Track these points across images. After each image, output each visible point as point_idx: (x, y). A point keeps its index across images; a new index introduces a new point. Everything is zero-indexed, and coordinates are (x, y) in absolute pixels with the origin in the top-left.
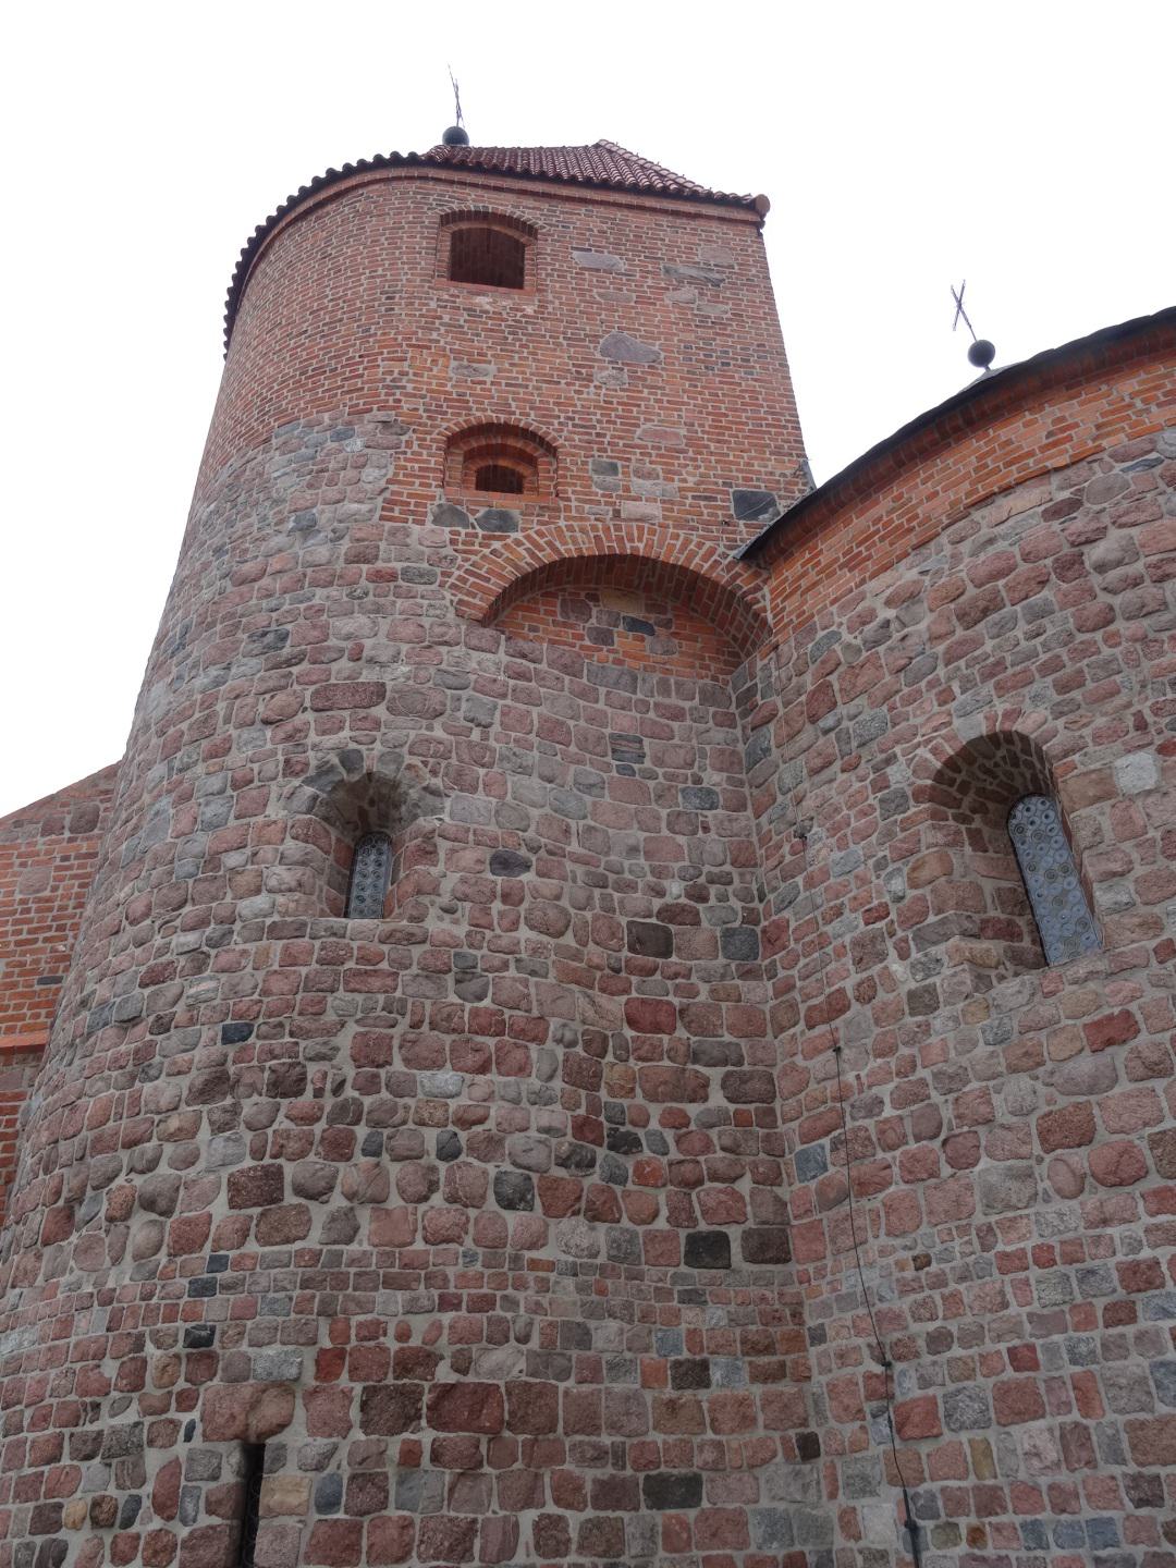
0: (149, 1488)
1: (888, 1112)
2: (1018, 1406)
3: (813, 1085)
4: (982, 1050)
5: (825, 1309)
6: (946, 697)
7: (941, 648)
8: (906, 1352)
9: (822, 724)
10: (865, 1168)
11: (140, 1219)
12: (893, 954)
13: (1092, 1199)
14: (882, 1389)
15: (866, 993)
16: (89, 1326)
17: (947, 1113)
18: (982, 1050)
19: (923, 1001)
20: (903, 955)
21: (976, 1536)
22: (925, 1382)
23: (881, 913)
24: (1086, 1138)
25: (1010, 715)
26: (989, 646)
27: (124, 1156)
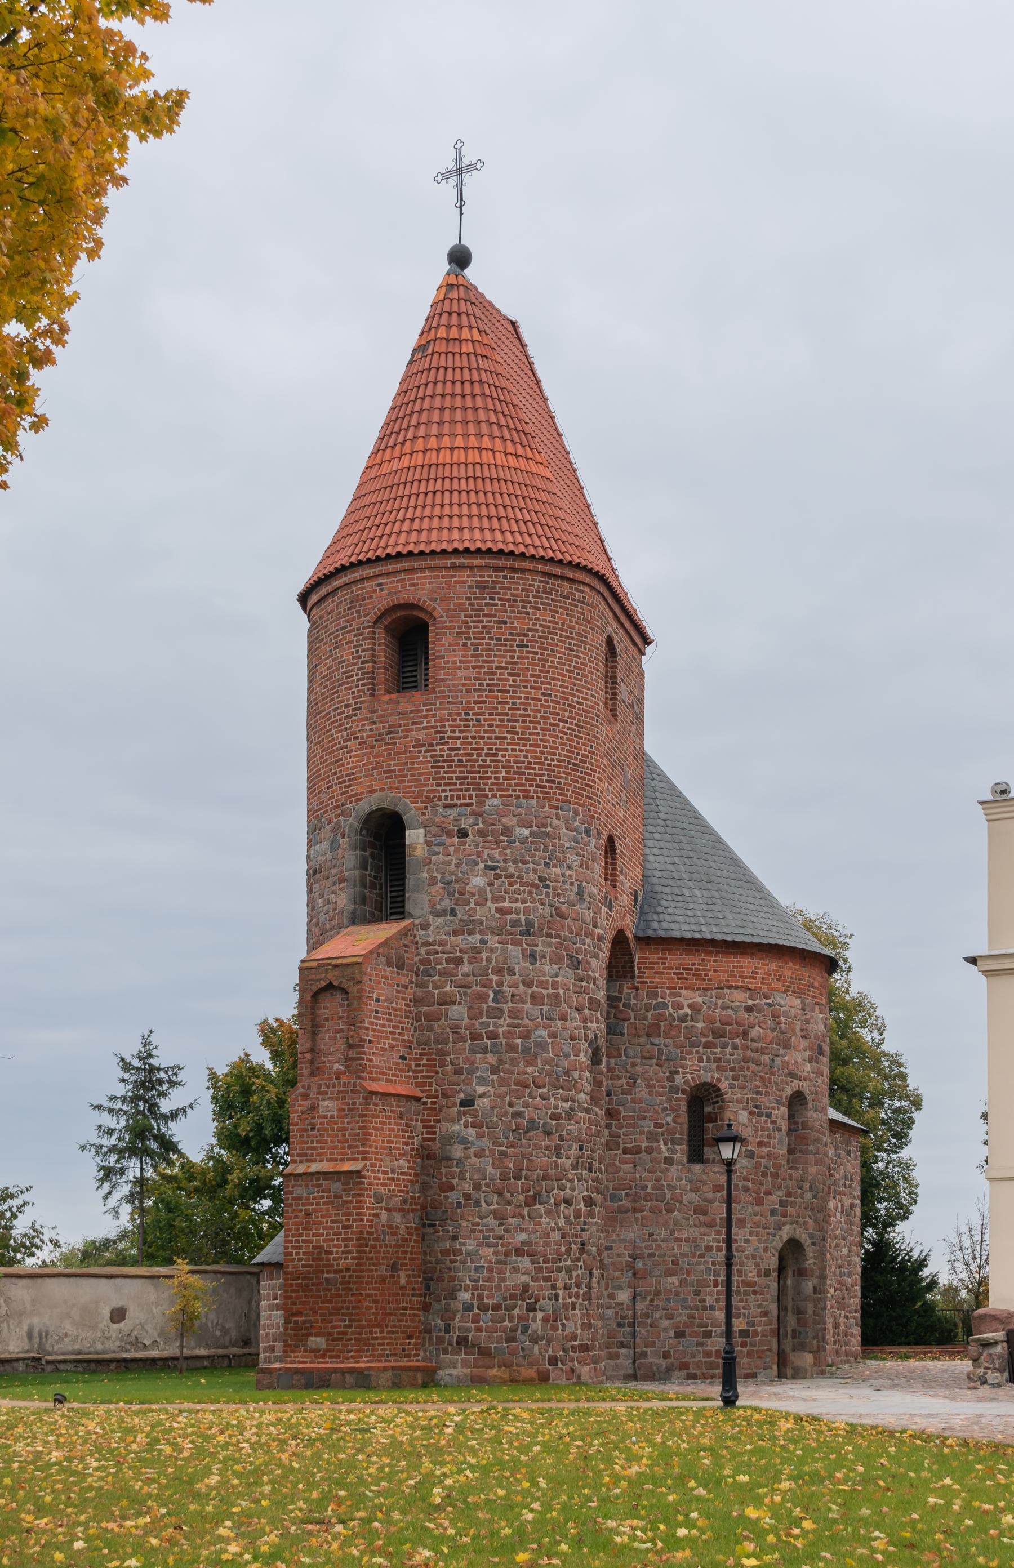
0: (573, 1281)
1: (649, 1190)
2: (670, 1273)
3: (621, 1173)
4: (684, 1182)
5: (614, 1241)
6: (700, 1060)
7: (704, 1040)
8: (640, 1256)
9: (653, 1040)
10: (638, 1205)
11: (563, 1205)
12: (662, 1142)
14: (631, 1266)
15: (649, 1151)
16: (556, 1236)
17: (668, 1196)
18: (684, 1182)
19: (669, 1161)
20: (666, 1144)
21: (652, 1300)
22: (644, 1265)
23: (661, 1126)
24: (705, 1214)
25: (719, 1080)
26: (718, 1050)
27: (556, 1183)
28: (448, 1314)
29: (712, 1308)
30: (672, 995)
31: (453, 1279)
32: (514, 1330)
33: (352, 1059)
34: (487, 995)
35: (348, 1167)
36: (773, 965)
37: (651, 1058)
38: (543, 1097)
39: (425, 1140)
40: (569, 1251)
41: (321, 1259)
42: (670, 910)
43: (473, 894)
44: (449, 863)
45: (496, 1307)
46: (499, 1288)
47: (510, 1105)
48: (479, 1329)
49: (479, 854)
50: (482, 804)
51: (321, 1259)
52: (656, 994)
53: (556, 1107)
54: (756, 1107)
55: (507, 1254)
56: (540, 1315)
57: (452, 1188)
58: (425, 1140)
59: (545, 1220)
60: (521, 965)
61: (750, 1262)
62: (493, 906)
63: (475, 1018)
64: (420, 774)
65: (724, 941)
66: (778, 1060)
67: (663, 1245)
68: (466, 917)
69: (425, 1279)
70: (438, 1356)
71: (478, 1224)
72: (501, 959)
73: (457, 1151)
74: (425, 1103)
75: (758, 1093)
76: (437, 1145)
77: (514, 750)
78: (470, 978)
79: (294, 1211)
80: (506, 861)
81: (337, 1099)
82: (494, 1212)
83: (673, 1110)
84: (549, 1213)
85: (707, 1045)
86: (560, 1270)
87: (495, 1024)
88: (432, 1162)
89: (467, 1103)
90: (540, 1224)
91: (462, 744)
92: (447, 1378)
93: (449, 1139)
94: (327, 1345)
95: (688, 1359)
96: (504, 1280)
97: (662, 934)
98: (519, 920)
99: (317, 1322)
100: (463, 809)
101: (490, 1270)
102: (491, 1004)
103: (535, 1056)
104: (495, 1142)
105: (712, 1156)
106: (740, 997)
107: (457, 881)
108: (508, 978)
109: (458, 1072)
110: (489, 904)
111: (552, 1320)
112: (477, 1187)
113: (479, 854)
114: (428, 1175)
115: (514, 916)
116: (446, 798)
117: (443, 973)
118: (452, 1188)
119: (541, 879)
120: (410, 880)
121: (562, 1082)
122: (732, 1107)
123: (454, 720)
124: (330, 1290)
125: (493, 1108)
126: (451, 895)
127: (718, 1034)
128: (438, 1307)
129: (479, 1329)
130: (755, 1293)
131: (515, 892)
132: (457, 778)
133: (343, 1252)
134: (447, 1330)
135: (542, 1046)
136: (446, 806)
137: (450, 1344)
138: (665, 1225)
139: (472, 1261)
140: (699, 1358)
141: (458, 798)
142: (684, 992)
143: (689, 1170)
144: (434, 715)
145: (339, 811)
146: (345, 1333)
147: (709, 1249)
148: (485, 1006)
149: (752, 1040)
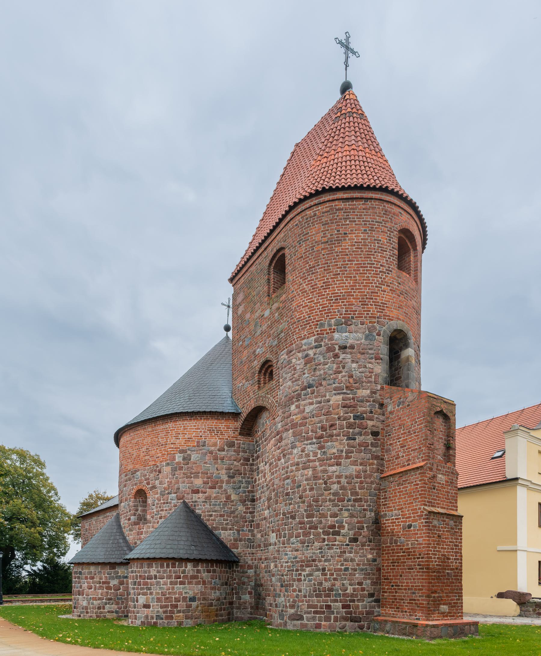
51: (445, 562)
94: (449, 610)
124: (449, 579)
145: (374, 320)
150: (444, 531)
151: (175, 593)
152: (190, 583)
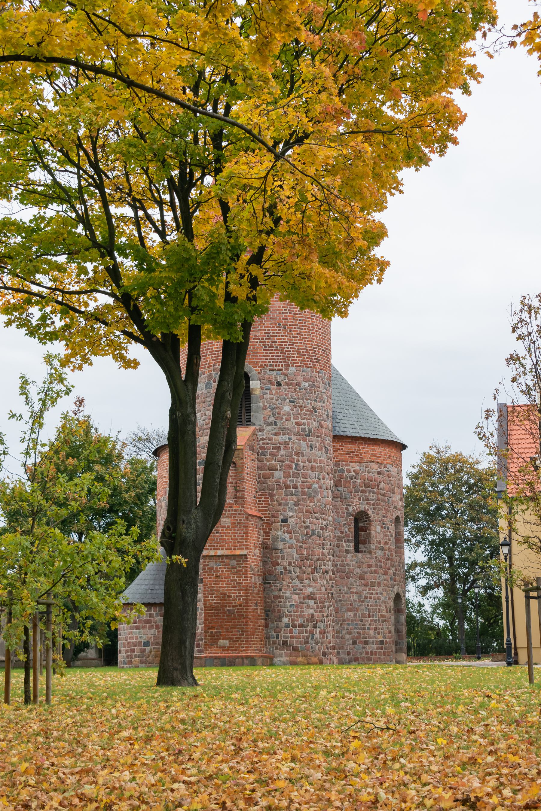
2: (349, 610)
6: (360, 500)
7: (361, 489)
13: (363, 587)
19: (347, 551)
20: (345, 542)
21: (341, 624)
23: (342, 533)
24: (364, 580)
25: (368, 509)
26: (367, 494)
28: (278, 629)
29: (368, 629)
30: (346, 465)
31: (279, 611)
32: (308, 638)
33: (239, 497)
34: (292, 466)
35: (238, 552)
36: (387, 450)
37: (337, 498)
38: (317, 519)
39: (264, 539)
40: (328, 597)
41: (225, 600)
42: (342, 421)
43: (284, 415)
44: (272, 399)
45: (300, 626)
46: (301, 616)
47: (304, 522)
48: (293, 637)
49: (287, 395)
50: (287, 369)
51: (225, 600)
52: (339, 464)
53: (322, 524)
54: (384, 524)
55: (304, 599)
56: (318, 630)
57: (278, 564)
58: (264, 539)
59: (319, 581)
60: (306, 451)
61: (383, 605)
62: (294, 421)
63: (287, 478)
64: (258, 353)
65: (369, 438)
66: (390, 499)
67: (346, 595)
68: (281, 426)
69: (266, 611)
70: (273, 651)
71: (291, 583)
72: (298, 448)
73: (280, 545)
74: (264, 520)
75: (384, 517)
76: (270, 542)
77: (301, 343)
78: (284, 457)
79: (209, 575)
80: (299, 399)
81: (231, 517)
82: (298, 577)
83: (349, 525)
84: (320, 577)
85: (362, 492)
86: (324, 607)
87: (296, 481)
88: (268, 551)
89: (284, 521)
90: (317, 583)
91: (278, 339)
92: (279, 662)
93: (276, 539)
95: (358, 656)
96: (303, 612)
97: (342, 434)
98: (305, 429)
99: (223, 632)
100: (278, 372)
101: (297, 607)
102: (294, 470)
103: (314, 497)
104: (298, 541)
105: (364, 550)
106: (375, 466)
107: (277, 408)
108: (301, 458)
109: (280, 505)
110: (292, 420)
111: (323, 632)
112: (290, 564)
113: (287, 395)
114: (266, 557)
115: (303, 426)
116: (271, 366)
117: (272, 454)
118: (278, 564)
119: (314, 408)
120: (253, 406)
121: (323, 511)
122: (374, 524)
123: (273, 327)
125: (296, 523)
126: (274, 415)
127: (367, 486)
128: (272, 625)
129: (293, 637)
130: (386, 621)
131: (303, 414)
132: (276, 356)
133: (237, 596)
134: (277, 638)
135: (316, 492)
136: (270, 370)
137: (279, 644)
138: (346, 585)
139: (289, 602)
140: (363, 655)
141: (276, 366)
142: (351, 464)
143: (356, 557)
144: (264, 324)
146: (240, 638)
147: (366, 598)
148: (291, 471)
149: (381, 489)
150: (222, 571)
151: (133, 638)
152: (144, 627)
